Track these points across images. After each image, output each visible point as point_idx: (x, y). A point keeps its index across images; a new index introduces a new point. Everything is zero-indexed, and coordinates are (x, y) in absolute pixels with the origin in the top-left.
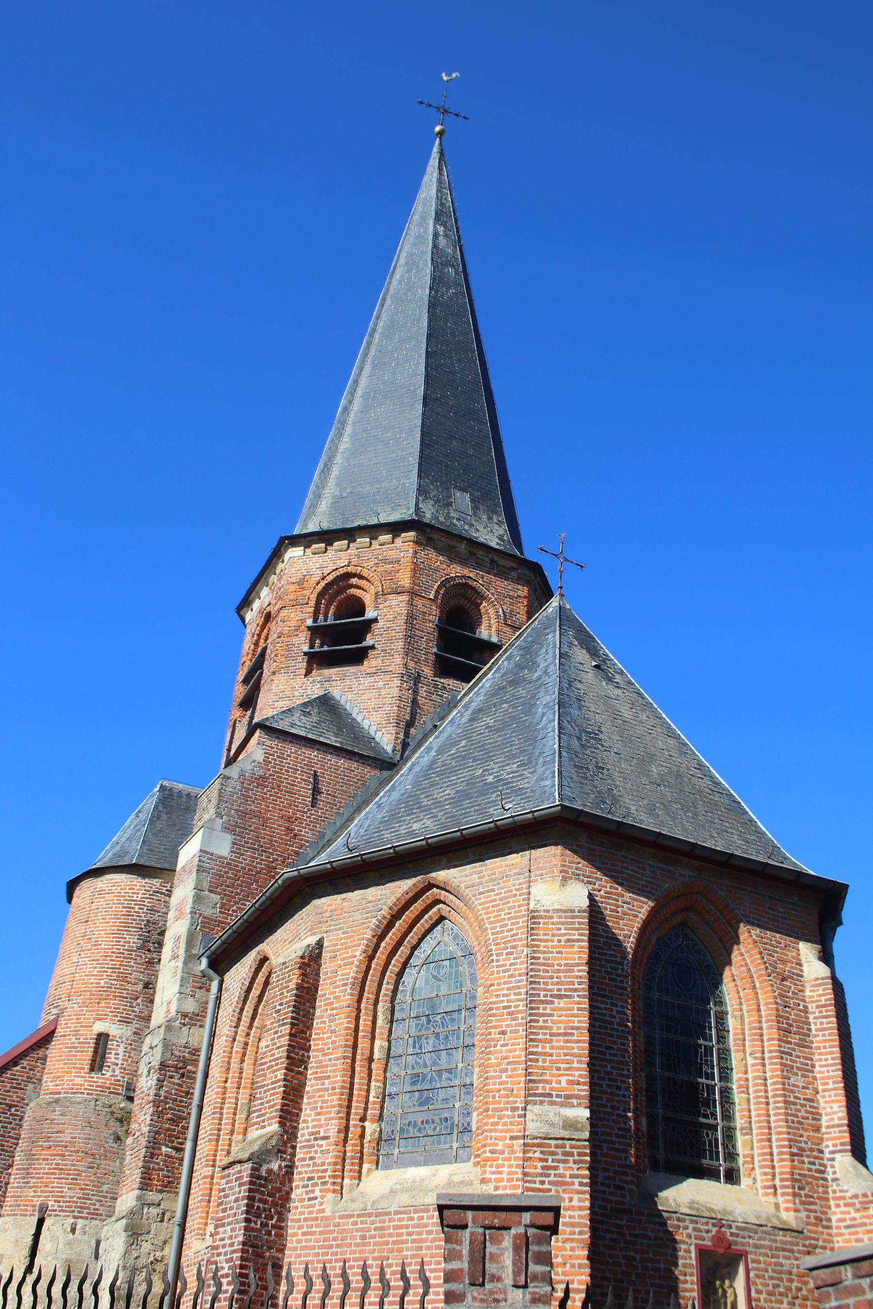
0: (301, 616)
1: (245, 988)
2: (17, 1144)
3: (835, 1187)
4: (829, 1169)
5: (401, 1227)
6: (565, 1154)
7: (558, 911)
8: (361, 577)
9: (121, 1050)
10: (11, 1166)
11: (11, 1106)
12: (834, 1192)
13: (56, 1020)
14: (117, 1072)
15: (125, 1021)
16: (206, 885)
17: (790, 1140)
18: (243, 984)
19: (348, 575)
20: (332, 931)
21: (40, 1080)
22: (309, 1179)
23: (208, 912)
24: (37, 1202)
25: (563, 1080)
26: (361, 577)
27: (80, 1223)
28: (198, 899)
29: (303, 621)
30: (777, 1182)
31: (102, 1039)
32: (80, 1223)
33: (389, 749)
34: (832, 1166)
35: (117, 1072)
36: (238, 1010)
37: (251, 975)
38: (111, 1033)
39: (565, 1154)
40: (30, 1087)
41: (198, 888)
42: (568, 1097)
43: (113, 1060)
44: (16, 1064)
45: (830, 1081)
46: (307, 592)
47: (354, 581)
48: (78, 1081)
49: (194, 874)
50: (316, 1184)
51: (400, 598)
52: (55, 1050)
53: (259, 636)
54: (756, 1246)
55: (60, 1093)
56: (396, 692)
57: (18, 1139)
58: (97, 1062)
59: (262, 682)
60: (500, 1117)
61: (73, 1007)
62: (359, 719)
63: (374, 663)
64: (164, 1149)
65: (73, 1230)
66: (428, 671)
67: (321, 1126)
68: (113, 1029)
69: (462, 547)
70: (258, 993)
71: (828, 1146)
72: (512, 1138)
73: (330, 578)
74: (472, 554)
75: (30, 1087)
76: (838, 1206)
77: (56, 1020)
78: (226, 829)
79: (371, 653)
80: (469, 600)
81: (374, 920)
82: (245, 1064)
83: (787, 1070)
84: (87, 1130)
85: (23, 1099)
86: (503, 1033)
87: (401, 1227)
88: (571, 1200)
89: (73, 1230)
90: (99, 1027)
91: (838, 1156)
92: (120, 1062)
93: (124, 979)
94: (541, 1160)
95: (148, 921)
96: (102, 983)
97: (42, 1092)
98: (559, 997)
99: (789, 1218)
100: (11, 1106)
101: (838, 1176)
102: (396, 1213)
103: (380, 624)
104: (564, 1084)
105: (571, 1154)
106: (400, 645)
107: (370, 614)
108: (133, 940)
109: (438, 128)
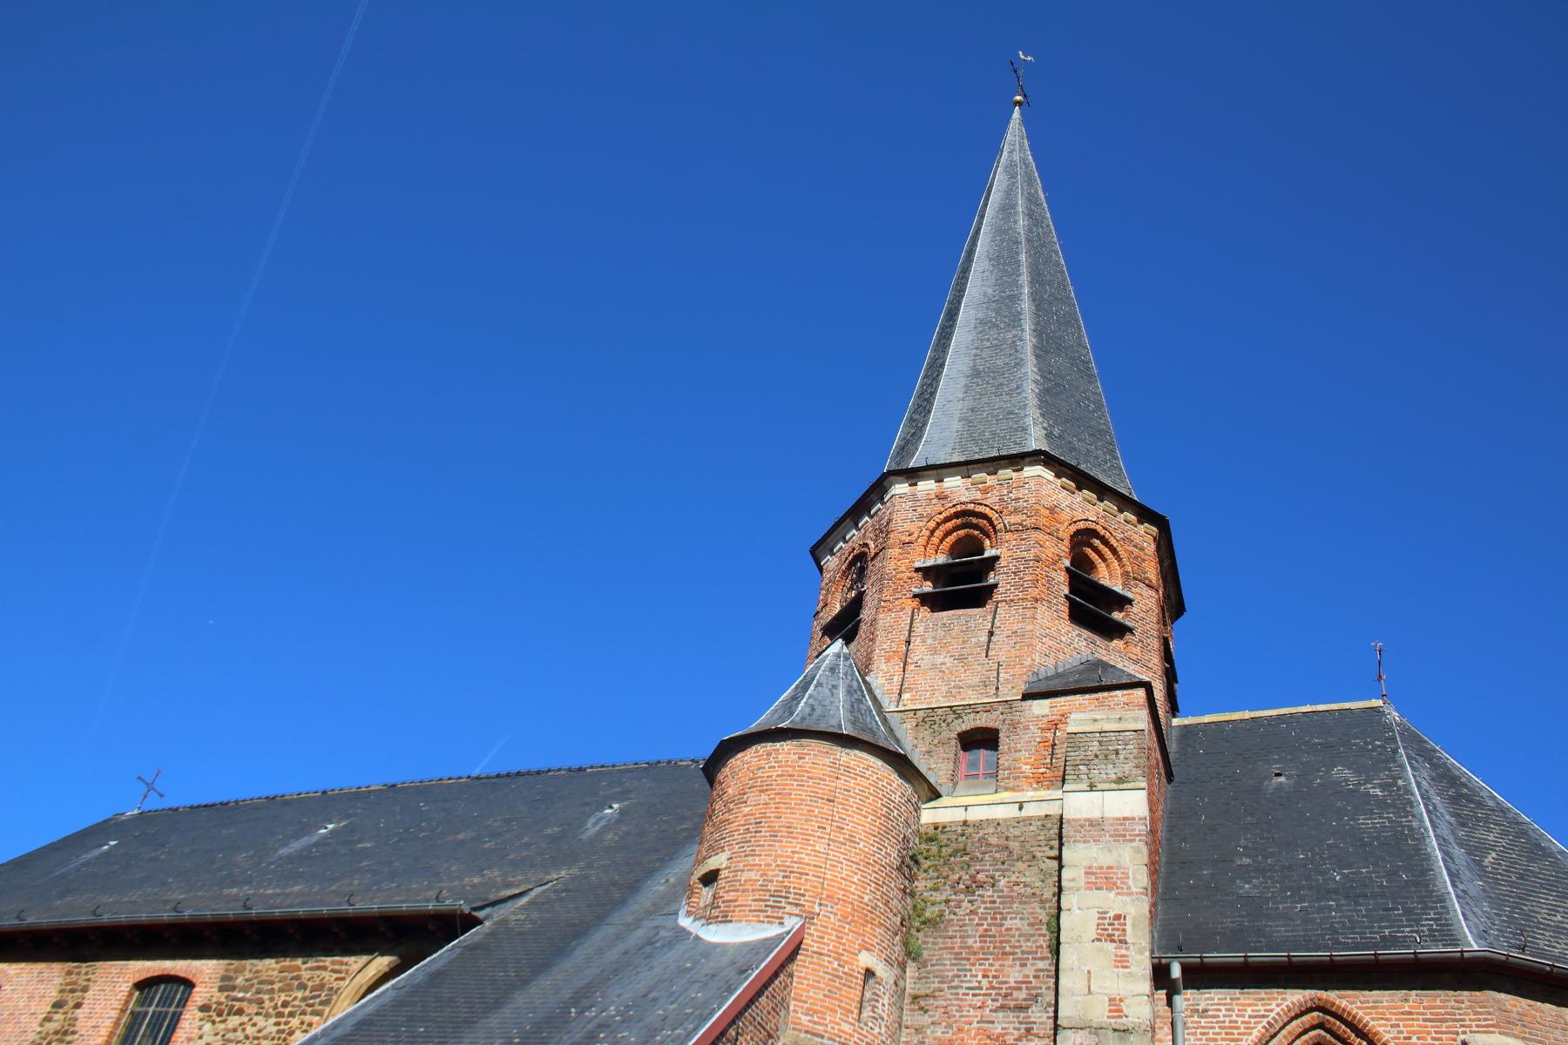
1: (1273, 1031)
8: (1105, 542)
9: (886, 1001)
19: (1093, 533)
26: (1105, 542)
40: (783, 1013)
47: (1097, 542)
48: (846, 1027)
52: (802, 968)
53: (938, 524)
61: (829, 917)
68: (881, 970)
79: (1128, 636)
90: (866, 959)
93: (887, 903)
96: (866, 898)
103: (1135, 610)
108: (894, 859)
109: (1018, 98)
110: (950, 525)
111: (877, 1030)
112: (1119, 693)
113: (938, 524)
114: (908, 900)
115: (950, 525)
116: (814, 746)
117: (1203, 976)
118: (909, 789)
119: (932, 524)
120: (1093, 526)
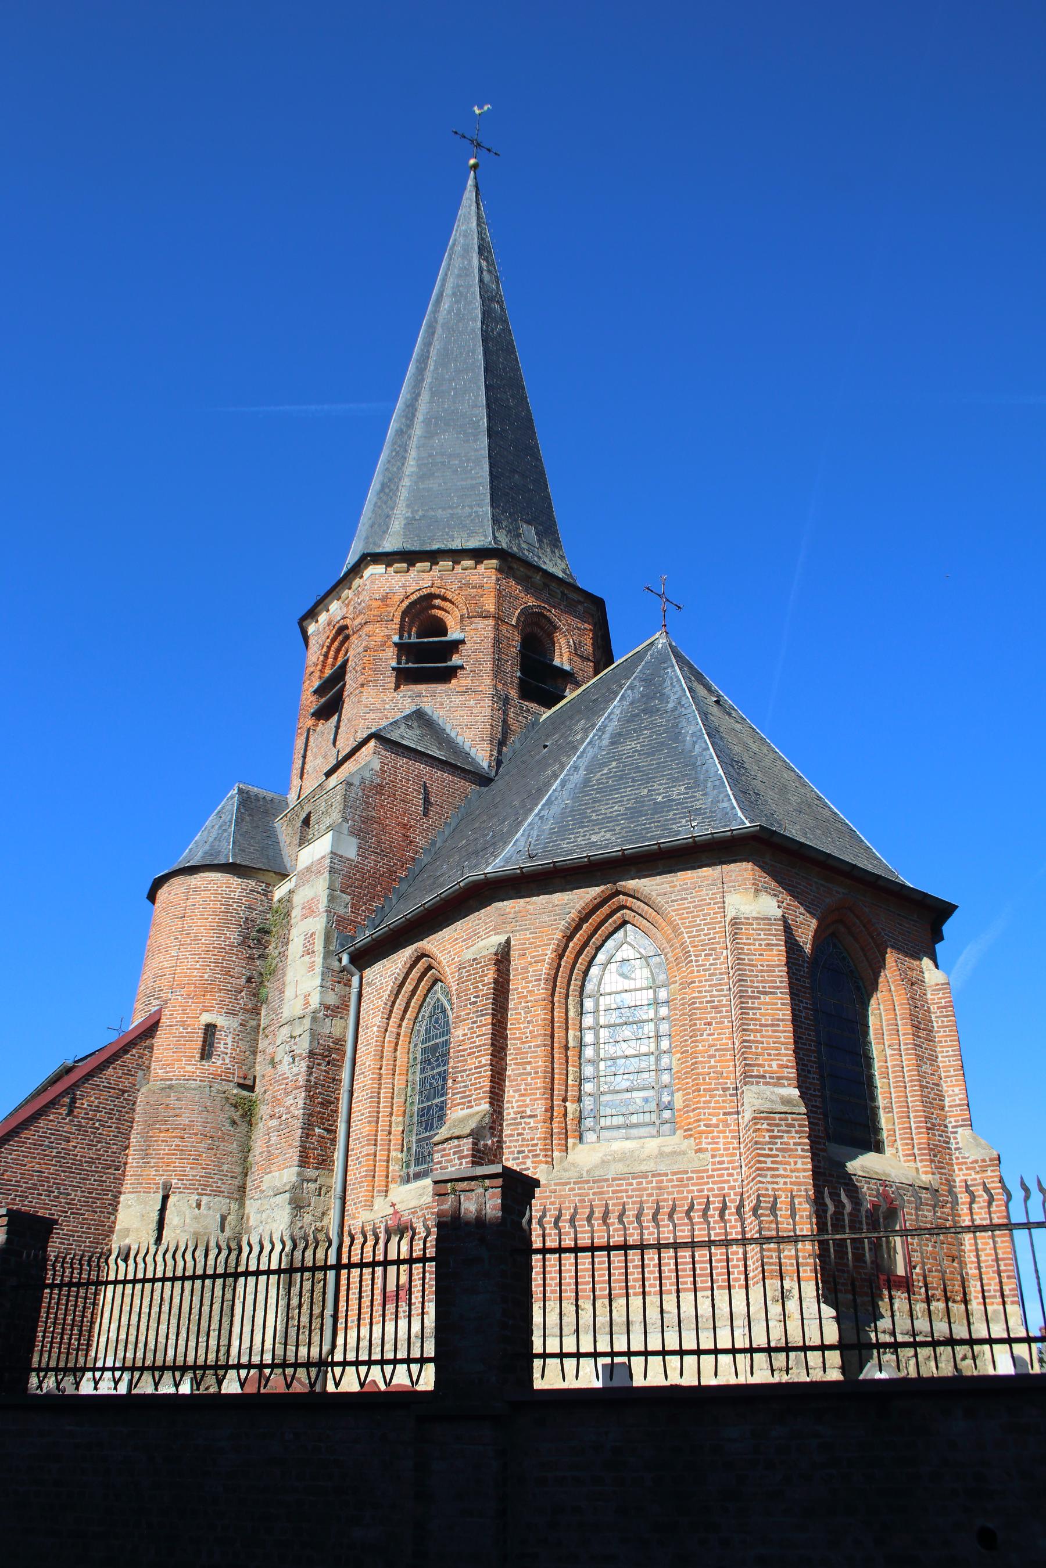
0: (387, 632)
1: (398, 982)
2: (132, 1127)
3: (957, 1155)
4: (952, 1140)
5: (621, 1191)
6: (787, 1125)
7: (757, 918)
8: (444, 599)
9: (229, 1040)
10: (127, 1147)
11: (124, 1092)
12: (957, 1158)
13: (160, 1010)
14: (227, 1061)
16: (338, 886)
17: (926, 1117)
18: (396, 979)
19: (432, 596)
20: (518, 931)
21: (149, 1068)
22: (519, 1152)
23: (341, 911)
24: (161, 1180)
25: (774, 1064)
26: (444, 599)
27: (205, 1199)
28: (332, 899)
29: (389, 637)
30: (916, 1151)
31: (210, 1030)
32: (205, 1199)
33: (485, 765)
34: (955, 1138)
35: (227, 1061)
36: (390, 1003)
37: (405, 971)
38: (218, 1024)
39: (787, 1125)
40: (140, 1073)
41: (331, 888)
42: (779, 1078)
43: (223, 1049)
44: (126, 1052)
45: (951, 1069)
46: (392, 609)
47: (437, 602)
48: (189, 1068)
49: (326, 875)
50: (527, 1157)
51: (486, 622)
52: (161, 1040)
53: (329, 648)
55: (171, 1080)
56: (487, 712)
57: (132, 1122)
58: (207, 1052)
59: (346, 693)
60: (712, 1096)
61: (177, 999)
62: (453, 735)
63: (463, 682)
64: (317, 1130)
65: (199, 1206)
66: (514, 694)
67: (527, 1106)
68: (221, 1021)
69: (538, 578)
70: (412, 988)
71: (951, 1122)
72: (725, 1114)
73: (414, 597)
74: (546, 585)
75: (140, 1073)
76: (960, 1169)
77: (160, 1010)
78: (352, 833)
79: (460, 673)
80: (542, 629)
81: (563, 922)
82: (398, 1053)
83: (919, 1058)
84: (205, 1115)
85: (134, 1085)
86: (709, 1024)
87: (621, 1191)
88: (796, 1163)
89: (199, 1206)
90: (206, 1018)
91: (960, 1130)
92: (229, 1051)
94: (768, 1131)
95: (247, 919)
97: (152, 1079)
98: (765, 993)
99: (926, 1178)
100: (124, 1092)
101: (960, 1145)
102: (614, 1179)
103: (467, 646)
104: (775, 1067)
105: (793, 1126)
106: (488, 667)
107: (454, 634)
108: (234, 937)
109: (472, 162)
110: (336, 643)
111: (219, 1062)
112: (364, 749)
113: (329, 648)
114: (258, 962)
115: (336, 643)
116: (176, 881)
117: (364, 957)
118: (252, 883)
119: (325, 650)
120: (428, 591)
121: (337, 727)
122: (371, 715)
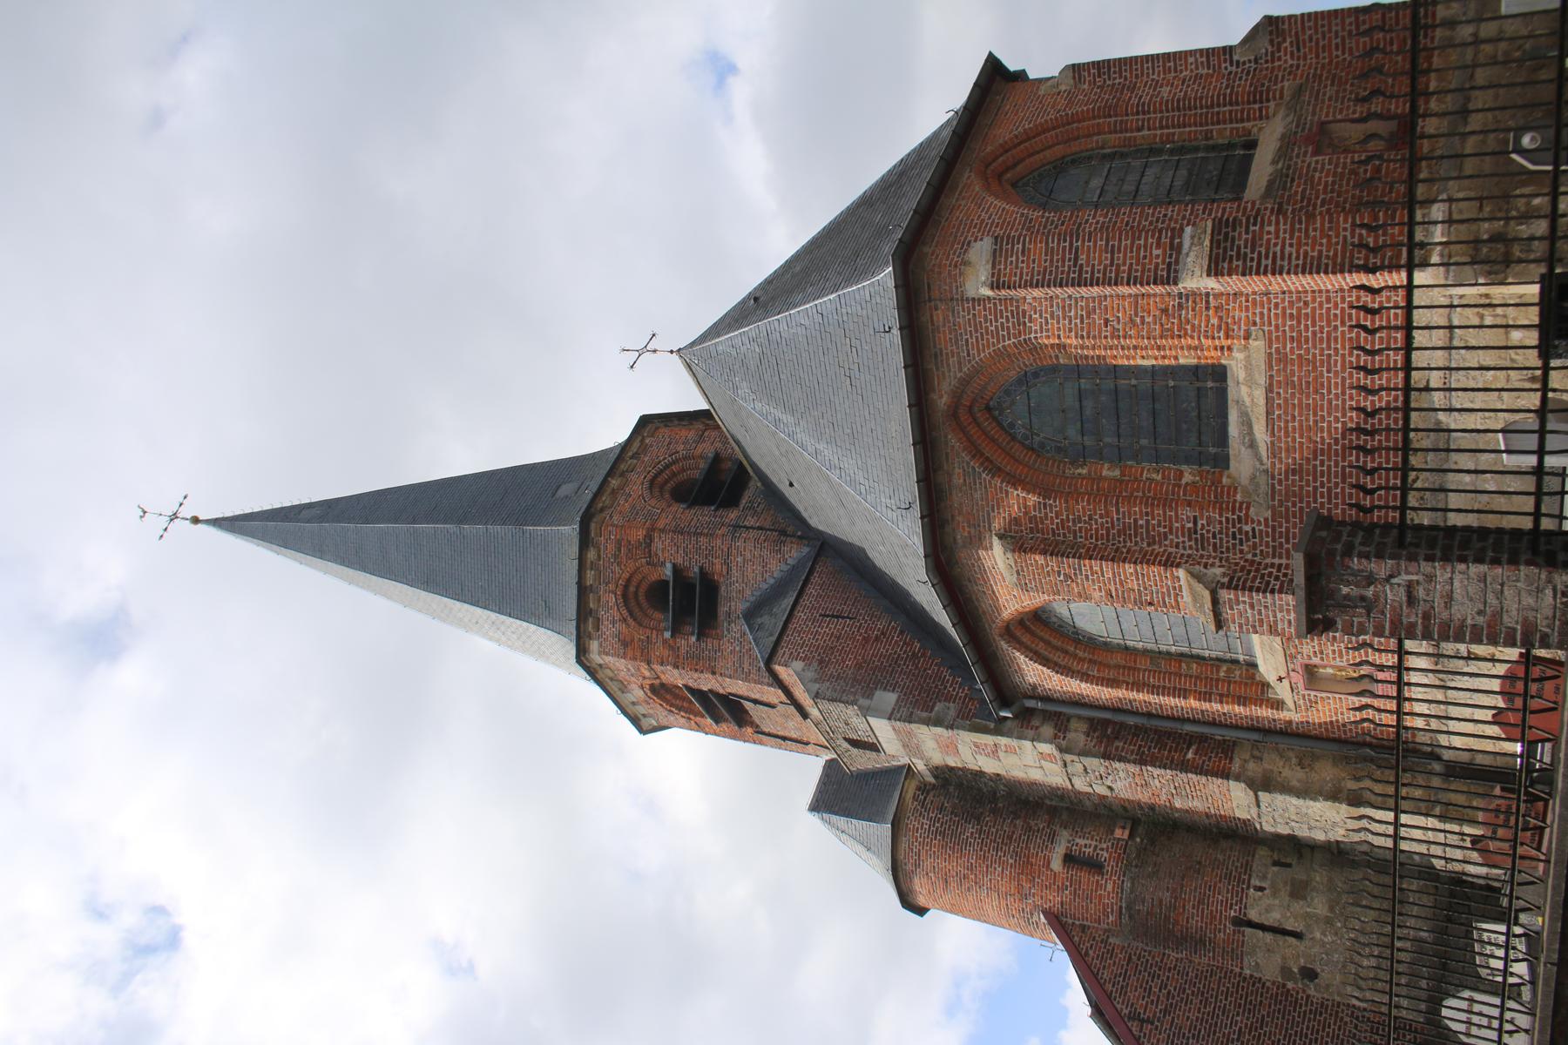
0: (660, 644)
5: (1286, 427)
6: (1226, 240)
7: (994, 267)
9: (1082, 842)
15: (1052, 838)
16: (925, 714)
22: (1234, 538)
23: (952, 713)
24: (1230, 928)
25: (1155, 252)
26: (629, 581)
27: (1255, 882)
28: (938, 723)
29: (665, 641)
31: (1069, 859)
32: (1255, 882)
33: (806, 550)
39: (1226, 240)
41: (927, 722)
42: (1172, 248)
46: (637, 637)
49: (913, 726)
50: (1240, 530)
54: (1314, 114)
58: (1095, 866)
59: (721, 691)
60: (1188, 322)
62: (772, 581)
63: (718, 567)
64: (1190, 755)
65: (1261, 889)
66: (733, 515)
67: (1183, 527)
68: (1059, 851)
72: (1207, 308)
74: (622, 474)
76: (1279, 59)
78: (870, 696)
80: (666, 482)
86: (1106, 322)
87: (1286, 427)
88: (1269, 233)
89: (1261, 889)
90: (1057, 864)
94: (1231, 261)
98: (1076, 259)
102: (1273, 435)
103: (680, 561)
104: (1159, 252)
105: (1226, 234)
107: (668, 571)
108: (971, 829)
121: (756, 702)
122: (746, 666)
